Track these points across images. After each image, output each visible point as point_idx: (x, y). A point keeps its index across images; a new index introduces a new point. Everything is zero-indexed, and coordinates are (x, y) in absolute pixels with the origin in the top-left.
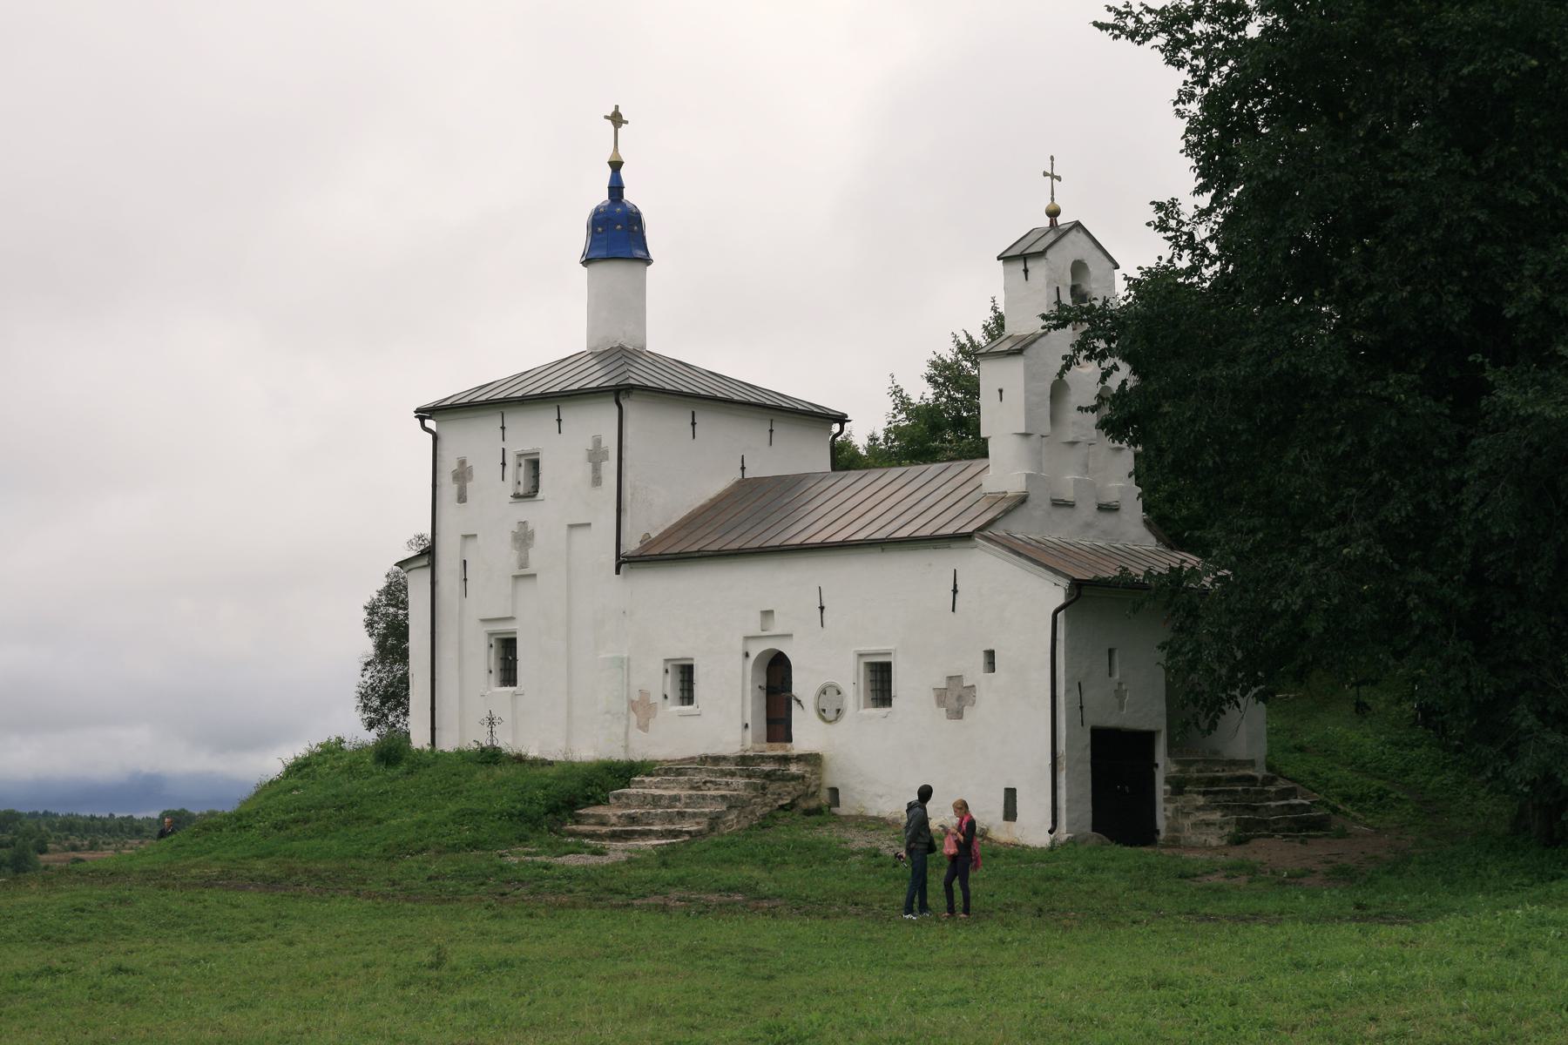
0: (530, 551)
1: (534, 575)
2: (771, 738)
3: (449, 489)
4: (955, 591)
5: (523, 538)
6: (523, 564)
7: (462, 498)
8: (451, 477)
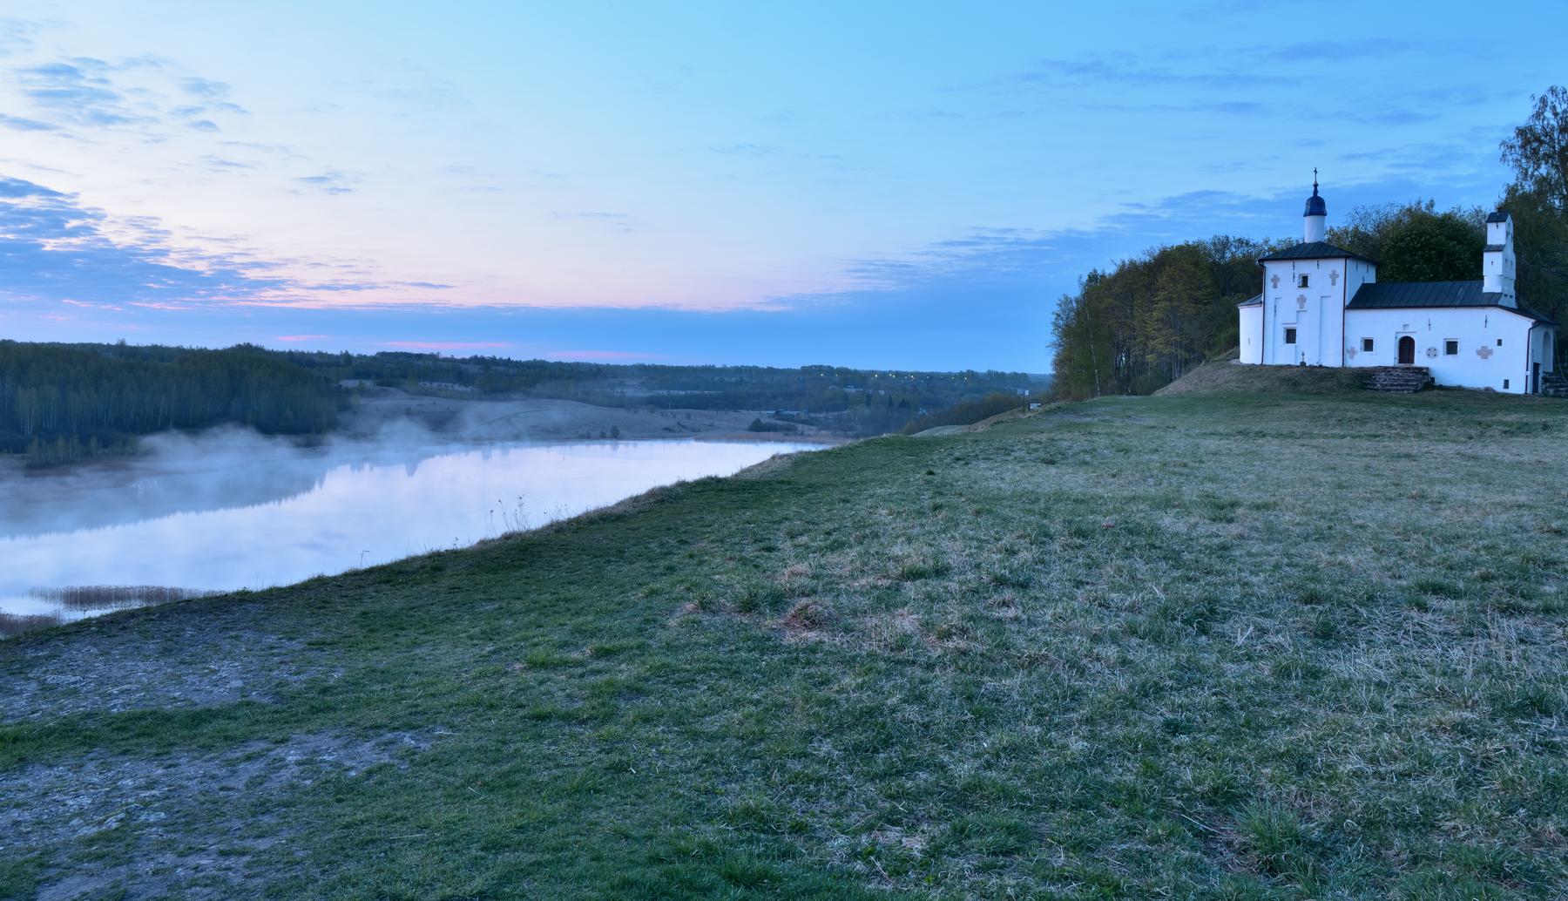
5: (1302, 300)
7: (1275, 287)
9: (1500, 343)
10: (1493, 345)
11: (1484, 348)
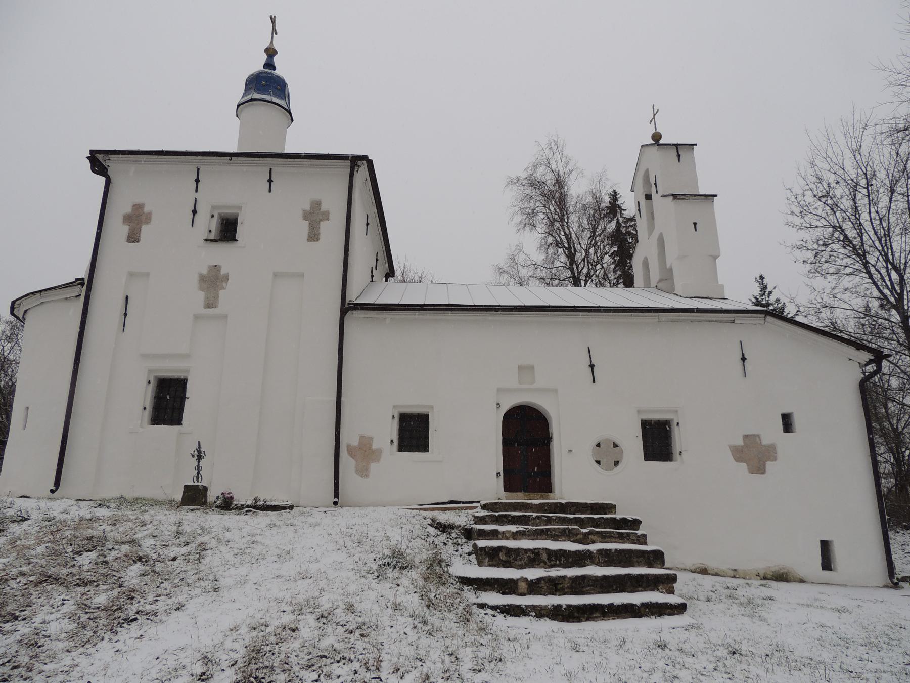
0: (222, 293)
1: (226, 317)
2: (507, 488)
3: (117, 229)
4: (744, 359)
6: (210, 304)
7: (133, 238)
8: (121, 219)
9: (787, 423)
10: (772, 433)
11: (751, 439)
